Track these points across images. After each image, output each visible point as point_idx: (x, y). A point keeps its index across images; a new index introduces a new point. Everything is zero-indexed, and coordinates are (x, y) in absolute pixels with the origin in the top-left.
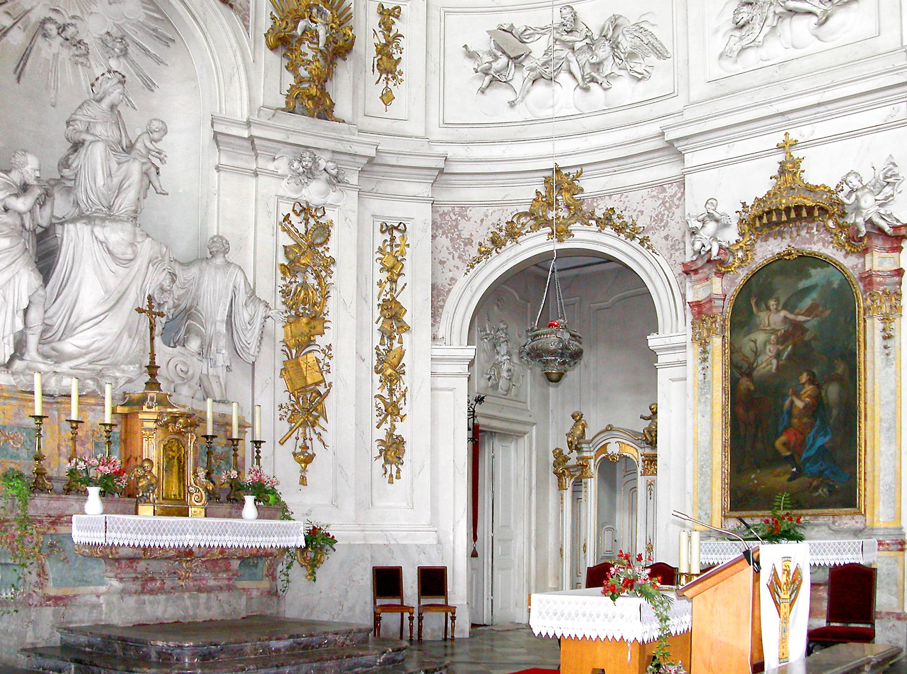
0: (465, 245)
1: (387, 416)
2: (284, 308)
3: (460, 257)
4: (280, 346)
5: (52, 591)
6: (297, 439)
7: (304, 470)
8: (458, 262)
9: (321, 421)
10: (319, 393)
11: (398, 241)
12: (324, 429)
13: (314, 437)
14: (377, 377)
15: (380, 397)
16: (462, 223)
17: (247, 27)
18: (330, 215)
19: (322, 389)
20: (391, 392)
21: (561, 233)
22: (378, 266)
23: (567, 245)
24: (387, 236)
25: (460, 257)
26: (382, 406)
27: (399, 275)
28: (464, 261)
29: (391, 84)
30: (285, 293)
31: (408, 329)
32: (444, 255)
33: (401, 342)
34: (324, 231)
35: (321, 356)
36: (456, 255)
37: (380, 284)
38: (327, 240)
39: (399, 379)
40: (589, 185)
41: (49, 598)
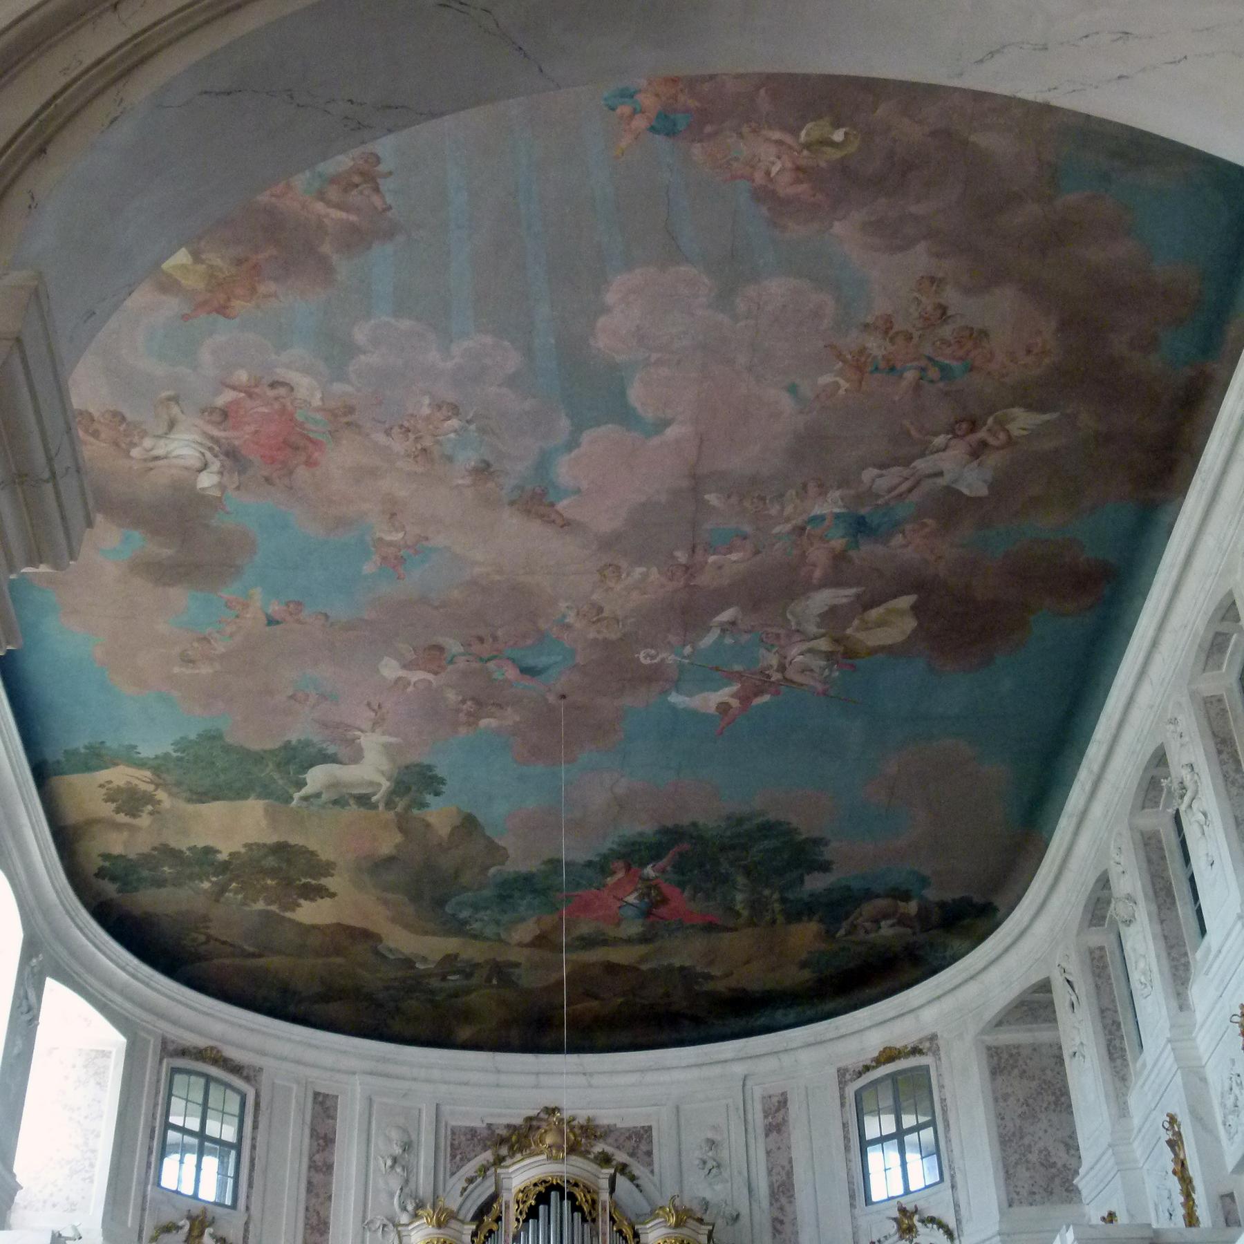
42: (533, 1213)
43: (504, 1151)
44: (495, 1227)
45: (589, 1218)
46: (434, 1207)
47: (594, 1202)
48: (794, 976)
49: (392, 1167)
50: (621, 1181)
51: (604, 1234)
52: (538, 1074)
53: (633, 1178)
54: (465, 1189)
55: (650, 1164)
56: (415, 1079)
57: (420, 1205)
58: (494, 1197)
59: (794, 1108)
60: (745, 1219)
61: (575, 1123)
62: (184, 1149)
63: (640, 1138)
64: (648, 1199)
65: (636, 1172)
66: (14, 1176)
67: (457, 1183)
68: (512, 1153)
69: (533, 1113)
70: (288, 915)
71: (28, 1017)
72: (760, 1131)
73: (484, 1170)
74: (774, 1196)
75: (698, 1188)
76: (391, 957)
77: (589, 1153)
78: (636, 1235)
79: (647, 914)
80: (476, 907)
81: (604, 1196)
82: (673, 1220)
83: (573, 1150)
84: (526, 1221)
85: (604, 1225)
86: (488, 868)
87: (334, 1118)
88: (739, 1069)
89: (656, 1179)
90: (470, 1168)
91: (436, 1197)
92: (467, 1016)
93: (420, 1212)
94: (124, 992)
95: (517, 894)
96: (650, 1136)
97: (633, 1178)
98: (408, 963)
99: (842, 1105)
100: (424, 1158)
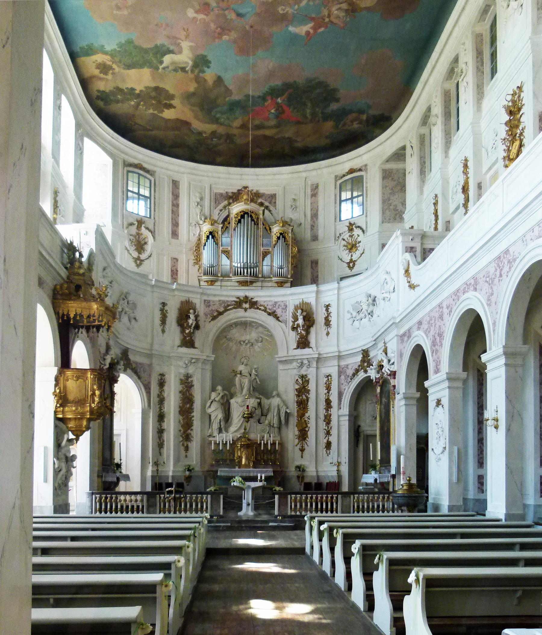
4: (296, 418)
9: (307, 439)
10: (306, 431)
11: (330, 380)
13: (305, 443)
14: (325, 423)
15: (325, 429)
17: (286, 326)
18: (309, 377)
19: (307, 429)
27: (330, 390)
30: (297, 402)
31: (332, 407)
33: (330, 411)
34: (308, 381)
35: (306, 419)
37: (325, 394)
39: (330, 423)
43: (231, 201)
45: (256, 224)
46: (210, 219)
48: (324, 142)
49: (197, 205)
50: (266, 211)
51: (261, 229)
52: (241, 175)
53: (270, 211)
54: (219, 213)
55: (275, 206)
56: (203, 176)
57: (206, 218)
58: (228, 216)
59: (321, 188)
60: (303, 225)
61: (253, 192)
62: (133, 198)
63: (272, 197)
64: (274, 217)
65: (271, 209)
66: (83, 206)
67: (217, 211)
68: (234, 202)
69: (240, 188)
71: (80, 152)
72: (310, 196)
73: (225, 207)
75: (290, 215)
77: (257, 202)
79: (277, 117)
80: (222, 113)
83: (252, 201)
84: (237, 224)
85: (261, 226)
86: (225, 98)
89: (277, 211)
90: (221, 206)
91: (210, 215)
92: (219, 154)
93: (206, 220)
94: (110, 143)
95: (235, 108)
96: (276, 197)
97: (270, 211)
98: (200, 133)
100: (207, 203)
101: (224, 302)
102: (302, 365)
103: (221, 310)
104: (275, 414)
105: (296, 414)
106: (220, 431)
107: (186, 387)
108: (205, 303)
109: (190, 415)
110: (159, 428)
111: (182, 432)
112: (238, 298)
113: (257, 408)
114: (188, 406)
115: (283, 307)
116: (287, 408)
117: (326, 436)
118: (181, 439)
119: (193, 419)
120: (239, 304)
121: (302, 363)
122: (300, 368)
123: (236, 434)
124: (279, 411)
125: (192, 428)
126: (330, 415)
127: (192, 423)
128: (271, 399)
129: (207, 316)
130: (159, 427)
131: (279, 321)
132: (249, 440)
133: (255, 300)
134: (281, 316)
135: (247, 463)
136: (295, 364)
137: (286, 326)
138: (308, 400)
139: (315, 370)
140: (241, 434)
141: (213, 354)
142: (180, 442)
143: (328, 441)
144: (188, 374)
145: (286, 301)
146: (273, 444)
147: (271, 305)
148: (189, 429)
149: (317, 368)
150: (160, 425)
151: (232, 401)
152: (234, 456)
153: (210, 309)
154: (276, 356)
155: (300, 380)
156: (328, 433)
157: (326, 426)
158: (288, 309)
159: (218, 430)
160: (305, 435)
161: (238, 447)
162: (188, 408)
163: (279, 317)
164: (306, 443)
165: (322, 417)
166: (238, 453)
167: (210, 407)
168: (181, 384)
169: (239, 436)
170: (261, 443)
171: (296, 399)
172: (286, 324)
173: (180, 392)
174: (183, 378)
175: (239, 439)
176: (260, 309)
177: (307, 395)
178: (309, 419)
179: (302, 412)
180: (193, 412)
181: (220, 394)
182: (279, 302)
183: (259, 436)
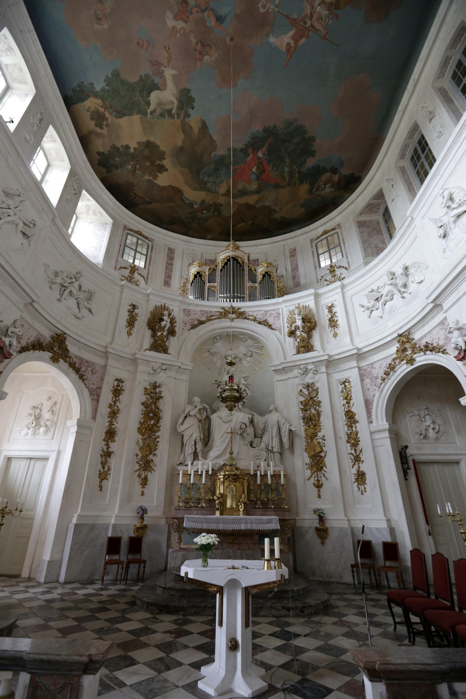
0: (376, 379)
1: (355, 462)
2: (304, 424)
3: (375, 385)
4: (304, 439)
5: (182, 546)
6: (315, 477)
7: (319, 491)
8: (374, 387)
9: (324, 468)
10: (321, 457)
11: (348, 386)
12: (325, 472)
13: (322, 476)
14: (349, 445)
15: (351, 454)
16: (373, 371)
18: (317, 385)
19: (322, 454)
20: (355, 450)
21: (411, 361)
22: (342, 398)
23: (416, 365)
24: (343, 386)
25: (375, 385)
26: (353, 458)
27: (350, 399)
28: (377, 386)
29: (336, 330)
30: (303, 419)
31: (357, 422)
32: (369, 386)
33: (356, 428)
34: (317, 391)
35: (320, 440)
36: (373, 384)
38: (317, 395)
39: (358, 444)
40: (417, 336)
41: (181, 549)
42: (226, 264)
44: (215, 268)
47: (243, 262)
70: (155, 181)
74: (293, 271)
76: (187, 202)
78: (255, 270)
81: (246, 261)
82: (266, 265)
87: (174, 254)
88: (282, 243)
98: (191, 204)
99: (312, 247)
101: (206, 312)
102: (306, 372)
103: (204, 319)
104: (274, 435)
105: (303, 434)
106: (195, 456)
107: (152, 398)
108: (184, 312)
109: (154, 435)
110: (105, 450)
111: (139, 457)
112: (223, 308)
113: (248, 425)
114: (152, 422)
115: (275, 315)
116: (291, 425)
117: (355, 464)
118: (137, 467)
119: (158, 440)
120: (224, 314)
121: (306, 369)
122: (304, 376)
123: (216, 460)
124: (279, 429)
125: (156, 452)
126: (357, 434)
127: (156, 445)
128: (267, 416)
129: (187, 324)
130: (105, 448)
131: (272, 329)
132: (237, 469)
133: (242, 310)
134: (274, 324)
135: (234, 506)
136: (296, 372)
137: (281, 334)
138: (319, 414)
139: (325, 376)
140: (225, 460)
141: (191, 363)
142: (135, 471)
143: (358, 471)
144: (155, 383)
145: (278, 309)
146: (276, 476)
147: (261, 315)
148: (150, 454)
149: (328, 374)
150: (107, 445)
151: (214, 417)
152: (214, 493)
153: (190, 317)
154: (270, 365)
155: (305, 391)
156: (357, 459)
157: (352, 449)
158: (281, 317)
159: (192, 455)
160: (321, 463)
161: (220, 479)
162: (152, 425)
163: (271, 325)
164: (324, 474)
165: (345, 438)
166: (220, 489)
167: (182, 423)
168: (145, 394)
169: (222, 463)
170: (256, 475)
171: (302, 415)
172: (280, 332)
173: (143, 404)
174: (148, 387)
175: (221, 468)
176: (248, 319)
177: (318, 408)
178: (324, 440)
179: (312, 430)
180: (159, 430)
181: (196, 407)
182: (270, 310)
183: (252, 463)
